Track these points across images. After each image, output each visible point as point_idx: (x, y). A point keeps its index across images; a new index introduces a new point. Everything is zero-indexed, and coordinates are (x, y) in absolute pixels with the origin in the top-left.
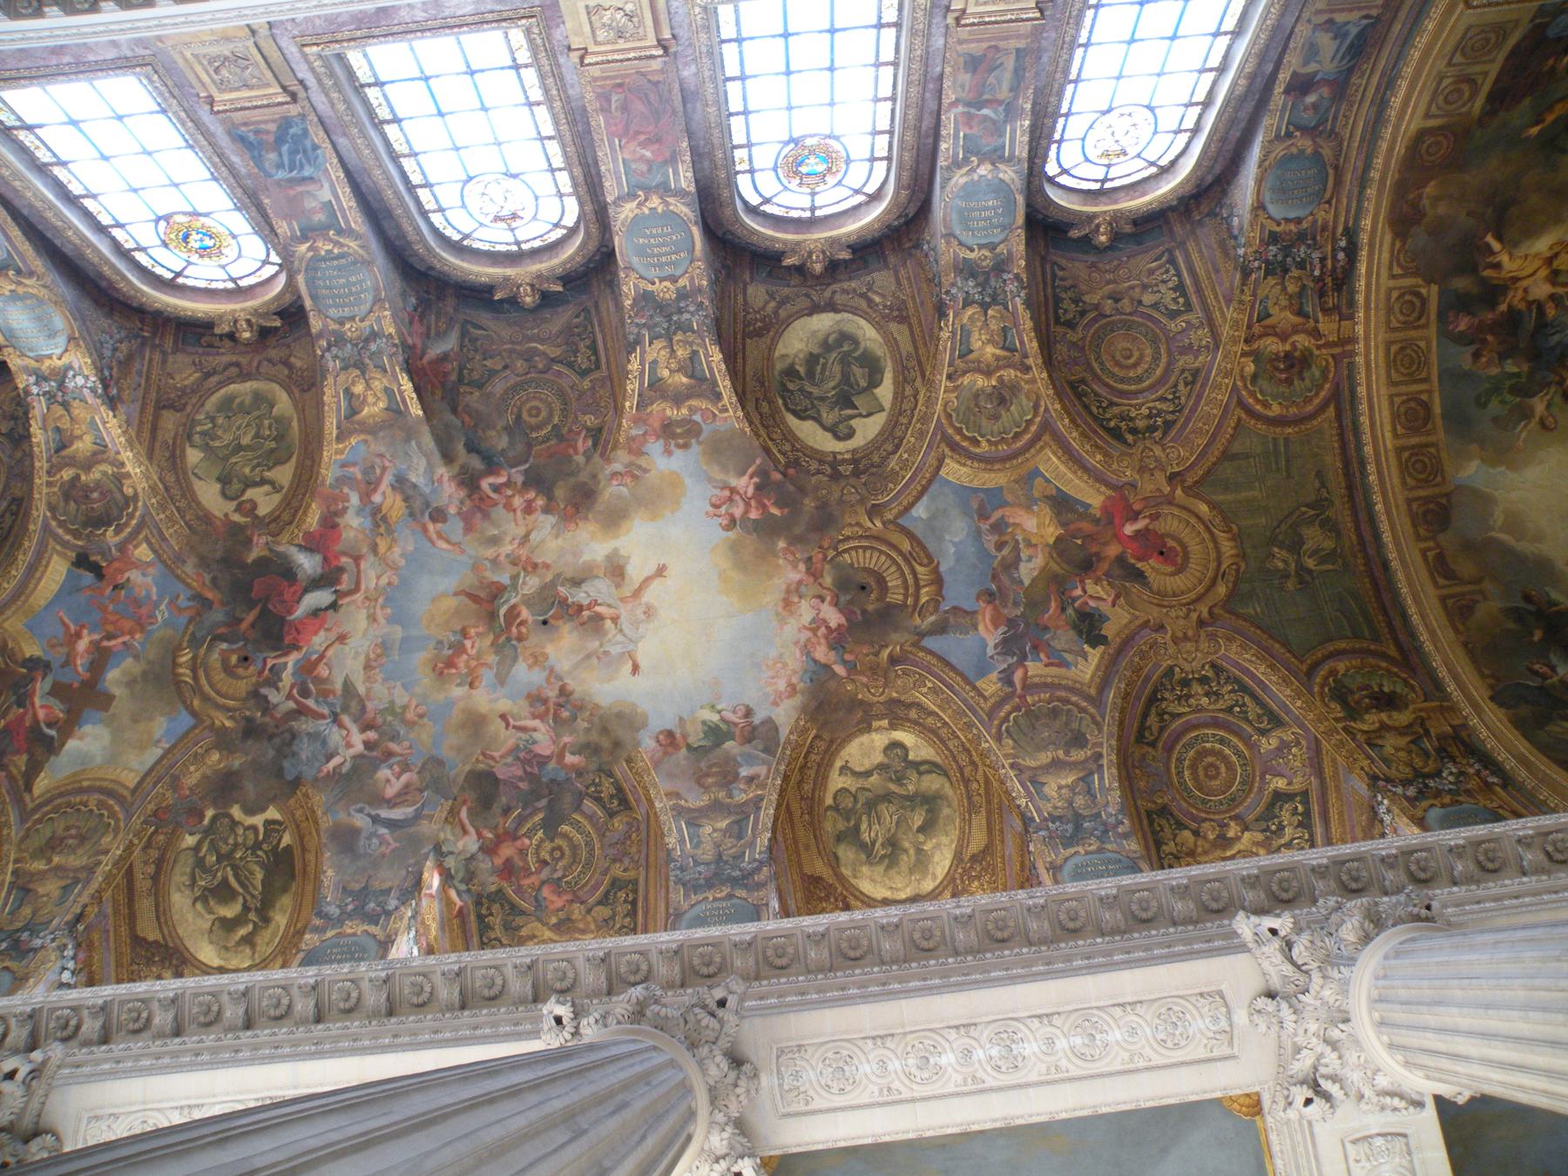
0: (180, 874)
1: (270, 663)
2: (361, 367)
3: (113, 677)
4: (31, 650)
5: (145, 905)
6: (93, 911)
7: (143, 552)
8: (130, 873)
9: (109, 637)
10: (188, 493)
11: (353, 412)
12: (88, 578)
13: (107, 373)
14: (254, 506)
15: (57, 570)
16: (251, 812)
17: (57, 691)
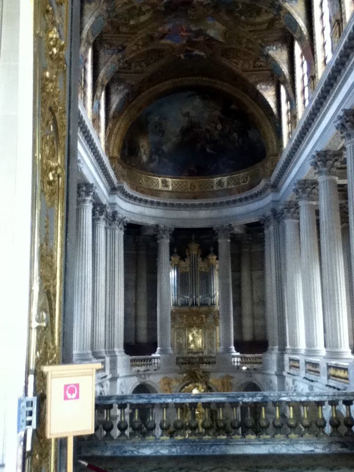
0: (252, 20)
1: (195, 3)
2: (114, 9)
3: (194, 29)
4: (185, 42)
5: (258, 27)
6: (260, 41)
7: (160, 29)
8: (250, 31)
9: (183, 30)
10: (144, 23)
11: (126, 3)
12: (167, 36)
13: (116, 51)
14: (148, 9)
15: (163, 41)
16: (239, 7)
17: (196, 37)
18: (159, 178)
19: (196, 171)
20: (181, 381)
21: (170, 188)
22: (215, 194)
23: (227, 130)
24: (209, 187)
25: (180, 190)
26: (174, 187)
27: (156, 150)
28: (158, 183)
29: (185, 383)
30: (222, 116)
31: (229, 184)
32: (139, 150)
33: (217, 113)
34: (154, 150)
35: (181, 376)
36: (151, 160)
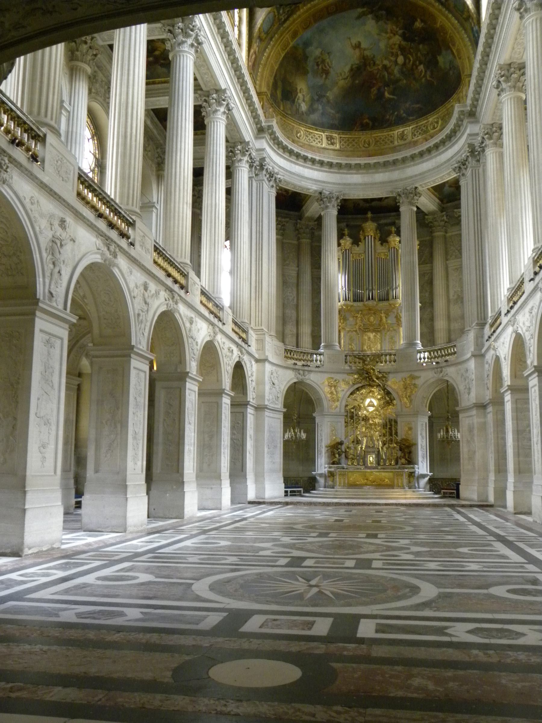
18: (322, 134)
19: (371, 124)
20: (351, 383)
21: (338, 147)
22: (395, 150)
23: (411, 62)
24: (388, 142)
25: (351, 149)
26: (343, 145)
27: (318, 95)
28: (322, 139)
29: (356, 386)
30: (404, 43)
31: (415, 135)
32: (297, 95)
33: (397, 39)
34: (316, 97)
35: (351, 378)
36: (311, 110)
